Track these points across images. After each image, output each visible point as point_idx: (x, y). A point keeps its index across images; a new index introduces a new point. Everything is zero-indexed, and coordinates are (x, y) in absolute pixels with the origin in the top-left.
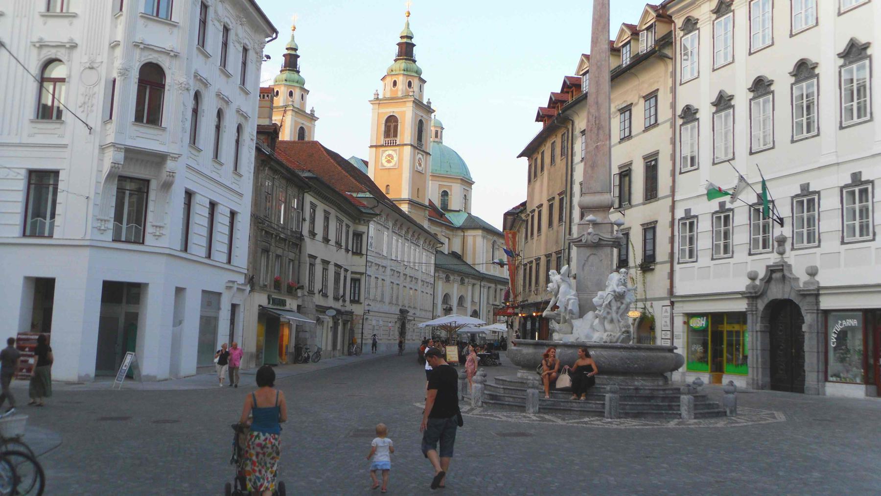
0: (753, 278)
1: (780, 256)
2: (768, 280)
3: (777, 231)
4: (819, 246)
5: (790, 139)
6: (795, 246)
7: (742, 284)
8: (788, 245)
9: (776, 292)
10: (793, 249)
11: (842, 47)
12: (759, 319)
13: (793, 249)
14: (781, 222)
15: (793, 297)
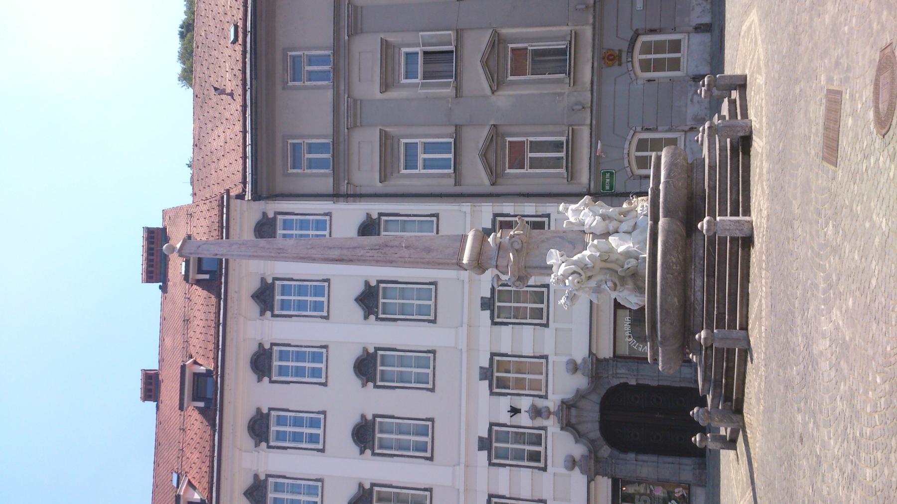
0: (572, 463)
1: (552, 416)
2: (579, 436)
3: (524, 419)
4: (546, 357)
5: (429, 393)
6: (543, 393)
7: (578, 479)
8: (541, 403)
9: (591, 412)
10: (545, 397)
11: (359, 312)
12: (622, 456)
13: (545, 397)
14: (515, 411)
15: (596, 398)
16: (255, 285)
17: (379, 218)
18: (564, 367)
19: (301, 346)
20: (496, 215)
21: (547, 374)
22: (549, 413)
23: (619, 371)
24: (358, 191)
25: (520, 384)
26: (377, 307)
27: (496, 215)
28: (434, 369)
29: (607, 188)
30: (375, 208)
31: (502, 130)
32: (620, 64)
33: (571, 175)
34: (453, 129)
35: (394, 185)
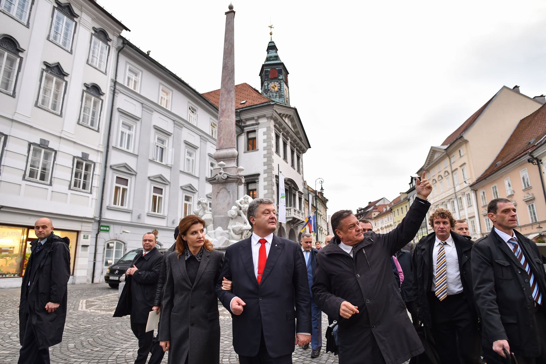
11: (52, 61)
17: (101, 99)
20: (95, 163)
24: (116, 94)
27: (95, 163)
29: (102, 228)
31: (133, 177)
33: (109, 209)
34: (136, 153)
35: (116, 114)
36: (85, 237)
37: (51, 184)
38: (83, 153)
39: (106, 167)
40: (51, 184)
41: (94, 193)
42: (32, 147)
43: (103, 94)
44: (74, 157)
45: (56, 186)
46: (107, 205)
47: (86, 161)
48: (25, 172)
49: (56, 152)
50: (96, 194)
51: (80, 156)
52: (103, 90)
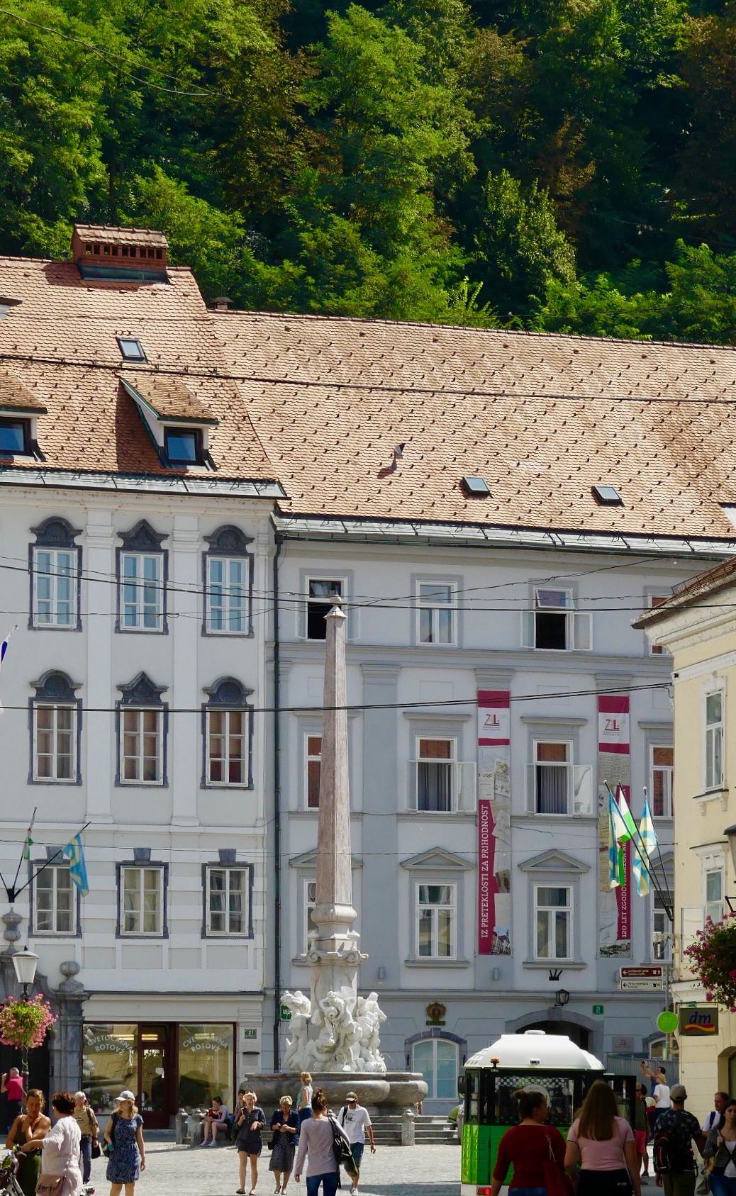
1: (8, 943)
4: (79, 934)
6: (35, 931)
8: (23, 928)
10: (31, 935)
11: (128, 675)
13: (31, 935)
16: (159, 525)
18: (70, 959)
19: (79, 592)
20: (251, 867)
21: (59, 937)
22: (12, 940)
23: (69, 1029)
25: (44, 902)
26: (134, 703)
27: (251, 867)
28: (58, 784)
30: (259, 700)
32: (428, 1023)
36: (251, 1034)
37: (166, 936)
38: (221, 852)
39: (277, 869)
40: (166, 936)
41: (258, 936)
42: (122, 870)
43: (251, 692)
44: (204, 866)
45: (175, 939)
46: (293, 956)
47: (229, 866)
48: (118, 922)
49: (166, 866)
50: (261, 940)
51: (216, 858)
52: (247, 682)
